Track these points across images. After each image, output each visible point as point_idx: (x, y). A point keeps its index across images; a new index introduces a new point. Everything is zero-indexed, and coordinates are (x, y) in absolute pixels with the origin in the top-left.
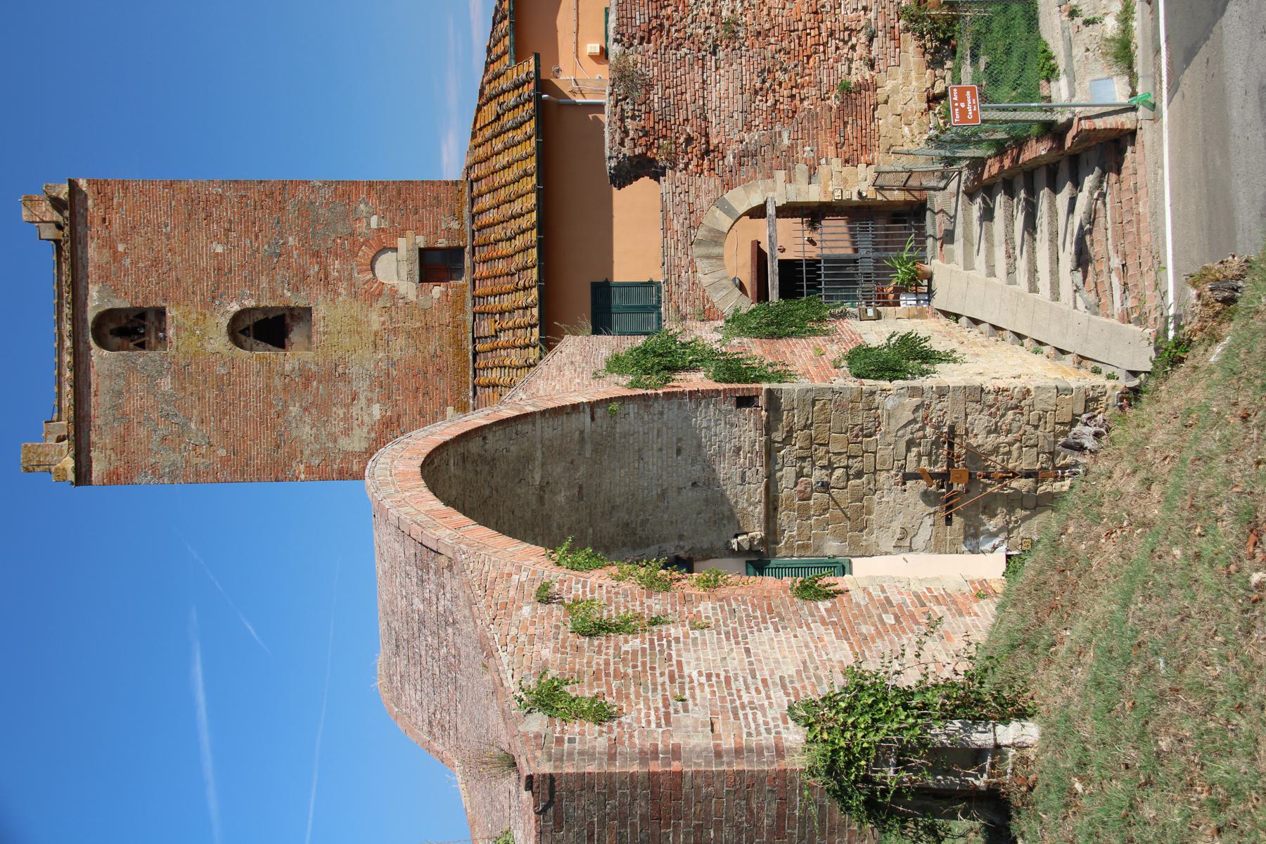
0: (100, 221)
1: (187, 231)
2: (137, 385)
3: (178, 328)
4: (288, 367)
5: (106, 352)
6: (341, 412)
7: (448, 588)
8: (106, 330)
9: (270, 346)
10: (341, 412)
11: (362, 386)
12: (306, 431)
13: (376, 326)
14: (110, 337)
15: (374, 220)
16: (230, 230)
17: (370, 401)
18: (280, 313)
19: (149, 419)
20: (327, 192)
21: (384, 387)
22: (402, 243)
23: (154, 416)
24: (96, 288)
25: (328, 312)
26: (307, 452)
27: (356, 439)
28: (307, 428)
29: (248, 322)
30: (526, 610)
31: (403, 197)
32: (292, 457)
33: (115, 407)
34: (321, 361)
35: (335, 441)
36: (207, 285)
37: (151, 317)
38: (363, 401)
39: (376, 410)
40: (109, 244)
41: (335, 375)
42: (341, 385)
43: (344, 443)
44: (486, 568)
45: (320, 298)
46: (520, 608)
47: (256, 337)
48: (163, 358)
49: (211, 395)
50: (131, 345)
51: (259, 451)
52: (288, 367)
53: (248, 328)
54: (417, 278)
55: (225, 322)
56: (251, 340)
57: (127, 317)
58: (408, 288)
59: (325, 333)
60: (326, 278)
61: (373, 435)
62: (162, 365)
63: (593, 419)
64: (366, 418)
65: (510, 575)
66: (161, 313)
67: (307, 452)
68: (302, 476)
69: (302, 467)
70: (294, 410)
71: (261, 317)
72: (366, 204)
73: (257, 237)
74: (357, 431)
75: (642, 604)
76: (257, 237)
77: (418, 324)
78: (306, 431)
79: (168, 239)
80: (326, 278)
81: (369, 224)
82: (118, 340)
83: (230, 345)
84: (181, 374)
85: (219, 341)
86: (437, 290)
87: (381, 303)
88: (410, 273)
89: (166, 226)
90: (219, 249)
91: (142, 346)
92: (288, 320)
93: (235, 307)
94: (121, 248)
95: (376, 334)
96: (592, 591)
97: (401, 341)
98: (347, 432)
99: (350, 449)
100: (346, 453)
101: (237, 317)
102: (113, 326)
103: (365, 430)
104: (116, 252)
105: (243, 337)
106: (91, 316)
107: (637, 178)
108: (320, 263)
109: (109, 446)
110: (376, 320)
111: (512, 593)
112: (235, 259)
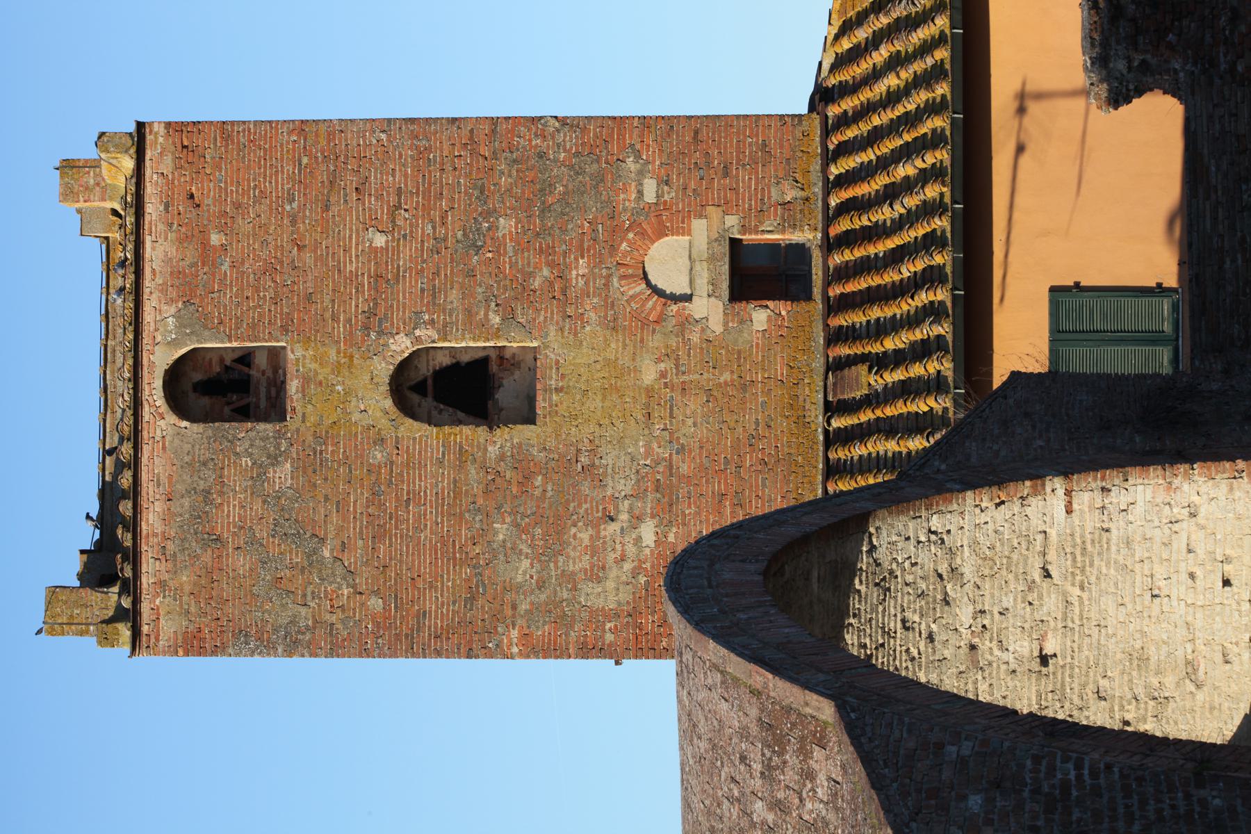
0: (183, 196)
1: (326, 208)
2: (237, 481)
3: (306, 381)
5: (185, 424)
6: (585, 536)
7: (821, 778)
9: (461, 415)
11: (624, 486)
12: (523, 569)
13: (649, 374)
14: (192, 396)
15: (650, 190)
16: (398, 207)
17: (637, 519)
18: (481, 354)
19: (253, 541)
20: (570, 139)
22: (699, 225)
23: (262, 533)
24: (173, 310)
25: (567, 354)
26: (524, 607)
27: (610, 585)
28: (526, 563)
29: (425, 369)
30: (975, 802)
31: (701, 147)
32: (497, 617)
33: (199, 516)
34: (552, 443)
35: (575, 589)
36: (358, 304)
37: (261, 361)
38: (624, 517)
39: (648, 533)
40: (193, 236)
41: (578, 467)
42: (585, 488)
44: (897, 734)
45: (552, 330)
46: (964, 798)
47: (437, 398)
48: (279, 435)
49: (358, 499)
50: (227, 410)
51: (438, 605)
52: (493, 451)
53: (425, 381)
54: (726, 294)
55: (383, 369)
56: (428, 403)
57: (222, 360)
58: (709, 308)
59: (558, 390)
60: (564, 291)
61: (642, 579)
62: (278, 446)
63: (1069, 511)
64: (631, 550)
65: (940, 746)
66: (276, 355)
67: (524, 607)
68: (515, 650)
69: (515, 633)
70: (502, 530)
71: (446, 361)
72: (638, 156)
73: (443, 218)
74: (613, 573)
75: (1188, 796)
76: (443, 218)
77: (727, 376)
78: (523, 569)
79: (294, 222)
80: (564, 291)
81: (640, 193)
82: (205, 401)
84: (311, 465)
85: (377, 403)
86: (760, 316)
88: (713, 283)
89: (291, 201)
90: (380, 240)
91: (244, 414)
92: (494, 367)
93: (402, 346)
94: (215, 239)
95: (649, 391)
96: (1094, 774)
97: (694, 404)
98: (596, 574)
99: (600, 603)
100: (593, 612)
101: (404, 367)
102: (198, 377)
103: (627, 566)
104: (205, 244)
105: (415, 398)
106: (159, 360)
107: (1140, 93)
108: (551, 265)
109: (187, 589)
111: (947, 774)
112: (407, 254)
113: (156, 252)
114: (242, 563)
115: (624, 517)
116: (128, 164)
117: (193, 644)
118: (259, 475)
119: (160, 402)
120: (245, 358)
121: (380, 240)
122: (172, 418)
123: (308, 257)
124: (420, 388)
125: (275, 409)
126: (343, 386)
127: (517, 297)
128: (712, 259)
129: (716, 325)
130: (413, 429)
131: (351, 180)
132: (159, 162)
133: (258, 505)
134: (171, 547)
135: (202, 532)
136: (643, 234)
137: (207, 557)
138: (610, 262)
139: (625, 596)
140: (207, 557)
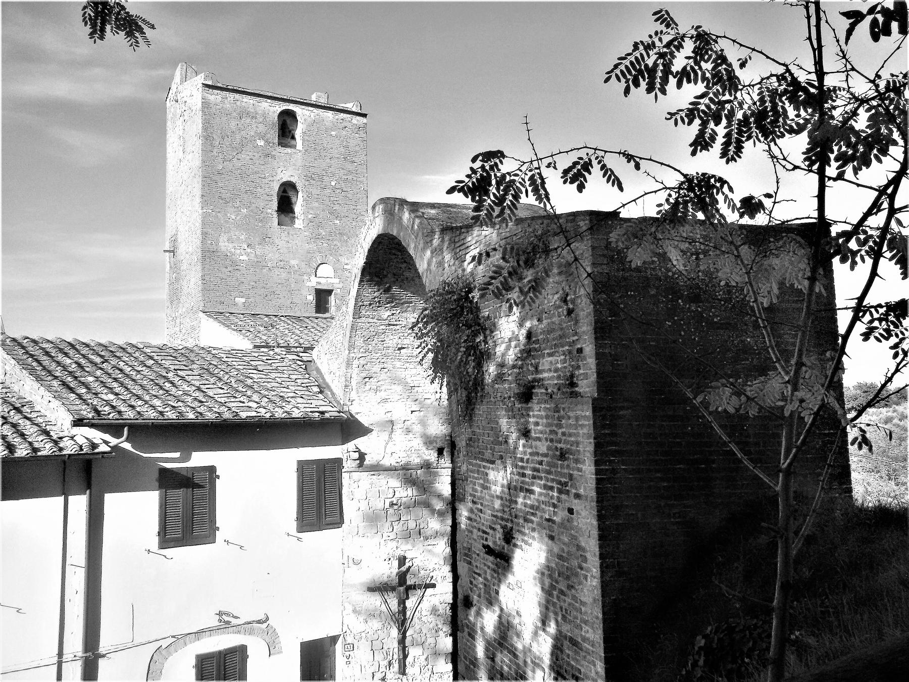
4: (269, 211)
8: (286, 118)
10: (242, 237)
21: (258, 264)
22: (337, 280)
27: (226, 244)
29: (291, 193)
37: (293, 142)
39: (244, 257)
40: (334, 127)
41: (265, 239)
43: (223, 238)
55: (293, 180)
58: (313, 283)
64: (238, 251)
71: (293, 199)
74: (231, 245)
83: (281, 182)
85: (285, 176)
86: (311, 298)
87: (303, 265)
94: (333, 133)
97: (284, 275)
99: (221, 240)
102: (288, 122)
110: (293, 262)
113: (330, 114)
114: (233, 124)
115: (249, 250)
116: (354, 109)
117: (206, 104)
118: (262, 137)
119: (284, 108)
120: (293, 138)
121: (333, 183)
122: (280, 110)
123: (328, 160)
124: (285, 191)
125: (280, 144)
126: (288, 166)
127: (314, 223)
128: (328, 285)
129: (308, 284)
130: (276, 188)
131: (350, 177)
132: (357, 120)
133: (252, 134)
134: (238, 103)
135: (243, 114)
136: (335, 263)
137: (234, 114)
138: (327, 253)
139: (223, 249)
140: (234, 114)
